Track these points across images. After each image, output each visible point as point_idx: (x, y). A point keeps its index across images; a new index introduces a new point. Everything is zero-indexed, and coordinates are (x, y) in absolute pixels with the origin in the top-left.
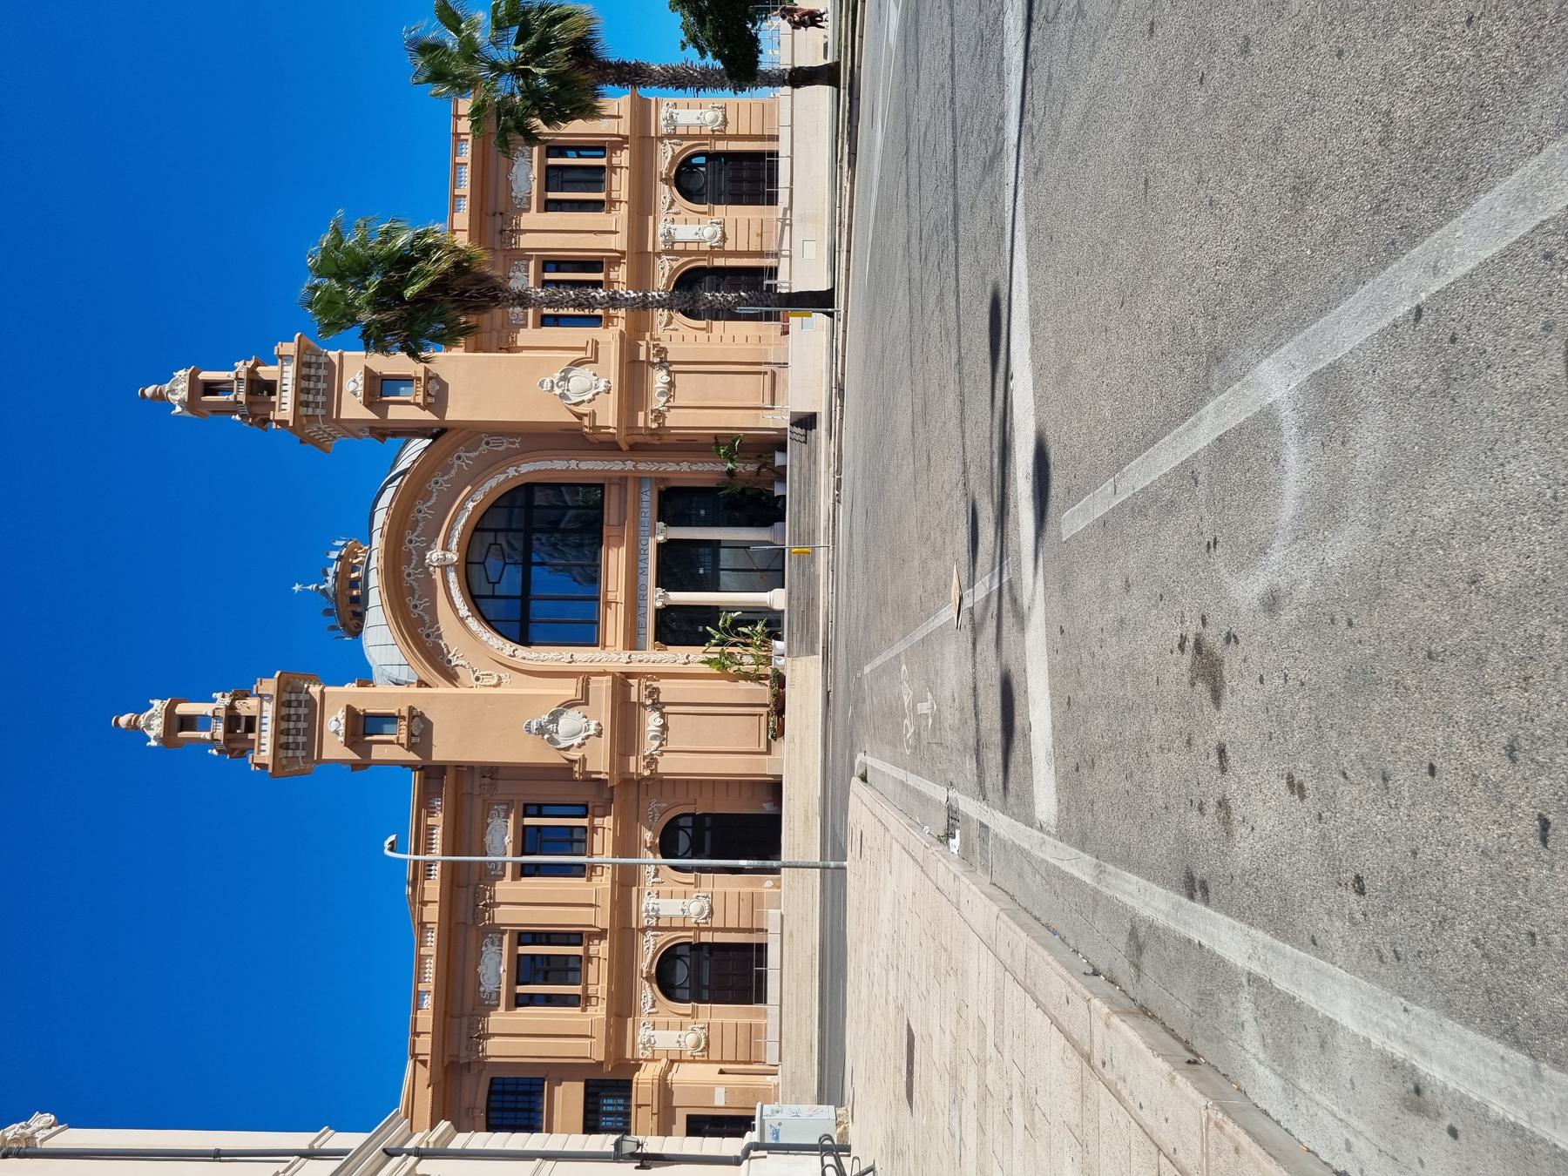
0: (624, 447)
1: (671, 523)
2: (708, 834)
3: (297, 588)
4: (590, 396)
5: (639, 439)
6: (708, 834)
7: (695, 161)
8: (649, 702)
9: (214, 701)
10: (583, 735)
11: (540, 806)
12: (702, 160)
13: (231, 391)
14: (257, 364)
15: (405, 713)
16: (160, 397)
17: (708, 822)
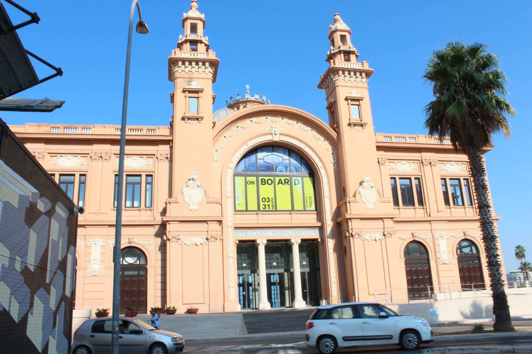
0: (339, 220)
1: (301, 246)
2: (135, 273)
3: (248, 87)
4: (364, 200)
5: (344, 227)
6: (135, 273)
7: (473, 248)
8: (209, 237)
9: (204, 36)
10: (190, 203)
11: (151, 183)
12: (474, 251)
13: (344, 44)
14: (357, 56)
15: (200, 115)
16: (335, 21)
17: (141, 273)
